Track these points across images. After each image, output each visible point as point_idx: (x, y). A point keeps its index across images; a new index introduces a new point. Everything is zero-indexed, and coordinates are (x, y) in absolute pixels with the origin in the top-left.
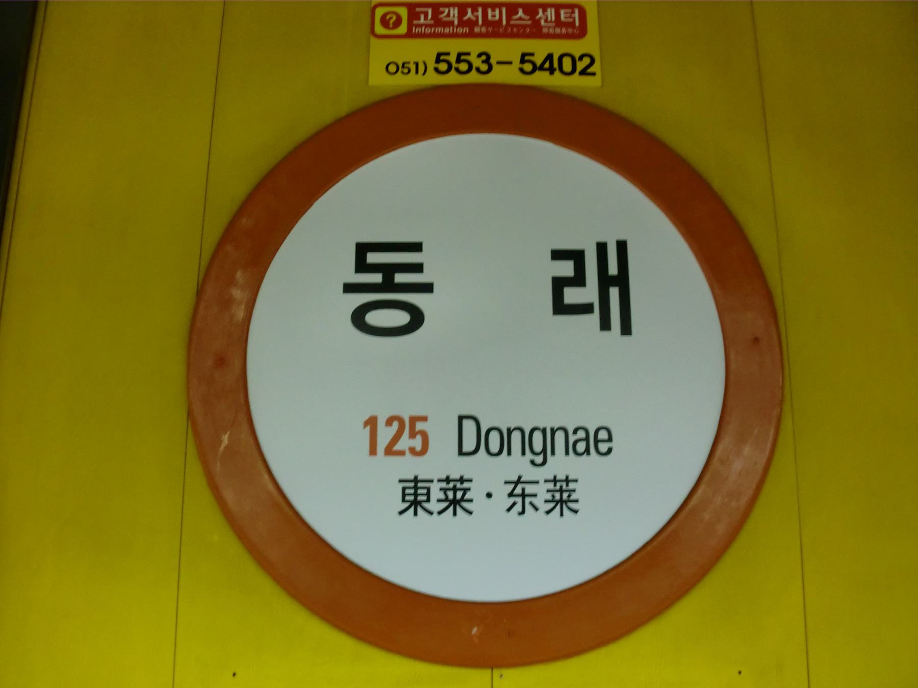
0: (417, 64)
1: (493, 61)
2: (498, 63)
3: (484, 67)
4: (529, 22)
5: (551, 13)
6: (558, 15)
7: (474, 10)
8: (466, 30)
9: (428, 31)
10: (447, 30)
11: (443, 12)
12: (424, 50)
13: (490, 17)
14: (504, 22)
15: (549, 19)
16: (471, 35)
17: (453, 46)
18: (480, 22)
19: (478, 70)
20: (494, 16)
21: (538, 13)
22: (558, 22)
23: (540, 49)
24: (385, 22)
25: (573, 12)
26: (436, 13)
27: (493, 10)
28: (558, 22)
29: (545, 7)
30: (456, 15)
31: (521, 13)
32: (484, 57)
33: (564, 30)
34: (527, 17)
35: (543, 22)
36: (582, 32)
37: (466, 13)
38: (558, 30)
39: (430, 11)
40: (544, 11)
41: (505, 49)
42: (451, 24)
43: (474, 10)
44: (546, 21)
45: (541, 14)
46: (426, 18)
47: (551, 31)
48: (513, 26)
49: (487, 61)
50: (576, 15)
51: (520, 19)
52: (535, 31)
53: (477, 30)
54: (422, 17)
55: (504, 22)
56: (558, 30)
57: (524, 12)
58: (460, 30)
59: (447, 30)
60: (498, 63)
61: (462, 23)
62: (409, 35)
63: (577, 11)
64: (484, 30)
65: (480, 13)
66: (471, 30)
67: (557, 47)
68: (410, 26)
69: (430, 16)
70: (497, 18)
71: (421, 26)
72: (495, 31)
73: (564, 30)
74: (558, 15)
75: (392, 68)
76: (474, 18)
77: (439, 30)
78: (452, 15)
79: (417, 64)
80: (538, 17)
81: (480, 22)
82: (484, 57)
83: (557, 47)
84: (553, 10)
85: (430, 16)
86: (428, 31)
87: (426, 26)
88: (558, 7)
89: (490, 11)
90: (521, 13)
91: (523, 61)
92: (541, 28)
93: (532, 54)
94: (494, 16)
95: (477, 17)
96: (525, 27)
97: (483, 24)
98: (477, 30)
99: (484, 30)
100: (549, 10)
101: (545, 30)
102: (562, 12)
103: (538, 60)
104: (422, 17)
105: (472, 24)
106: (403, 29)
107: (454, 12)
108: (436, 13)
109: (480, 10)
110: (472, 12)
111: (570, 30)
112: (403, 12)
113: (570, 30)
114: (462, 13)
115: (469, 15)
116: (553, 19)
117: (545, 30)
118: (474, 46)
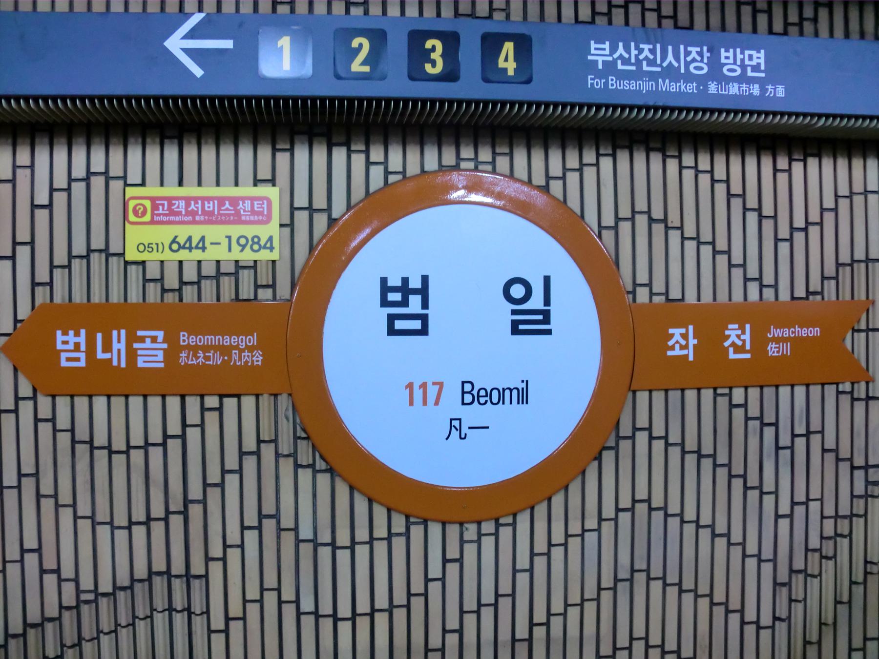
5: (248, 204)
6: (252, 205)
7: (196, 203)
8: (190, 218)
9: (165, 219)
10: (178, 219)
13: (207, 209)
16: (194, 222)
18: (200, 213)
22: (253, 212)
24: (136, 213)
26: (170, 205)
28: (253, 212)
29: (244, 199)
31: (227, 205)
38: (252, 218)
39: (166, 203)
43: (196, 203)
44: (244, 211)
45: (241, 206)
46: (163, 209)
47: (248, 218)
48: (222, 215)
51: (227, 209)
52: (237, 219)
53: (197, 218)
54: (161, 207)
56: (252, 218)
57: (230, 205)
58: (186, 219)
59: (178, 219)
61: (188, 213)
62: (152, 222)
64: (202, 218)
65: (199, 205)
66: (194, 218)
67: (249, 231)
68: (153, 215)
70: (211, 209)
71: (159, 215)
72: (211, 219)
74: (252, 205)
75: (141, 248)
77: (172, 218)
79: (157, 244)
81: (200, 213)
83: (249, 231)
86: (165, 219)
87: (164, 215)
90: (227, 205)
92: (240, 215)
94: (209, 207)
95: (197, 208)
96: (229, 215)
97: (202, 214)
98: (197, 218)
99: (202, 218)
101: (243, 218)
102: (255, 203)
104: (161, 207)
105: (194, 213)
106: (147, 218)
107: (182, 204)
108: (170, 205)
109: (200, 202)
112: (148, 204)
114: (188, 205)
115: (193, 206)
117: (243, 218)
118: (196, 232)
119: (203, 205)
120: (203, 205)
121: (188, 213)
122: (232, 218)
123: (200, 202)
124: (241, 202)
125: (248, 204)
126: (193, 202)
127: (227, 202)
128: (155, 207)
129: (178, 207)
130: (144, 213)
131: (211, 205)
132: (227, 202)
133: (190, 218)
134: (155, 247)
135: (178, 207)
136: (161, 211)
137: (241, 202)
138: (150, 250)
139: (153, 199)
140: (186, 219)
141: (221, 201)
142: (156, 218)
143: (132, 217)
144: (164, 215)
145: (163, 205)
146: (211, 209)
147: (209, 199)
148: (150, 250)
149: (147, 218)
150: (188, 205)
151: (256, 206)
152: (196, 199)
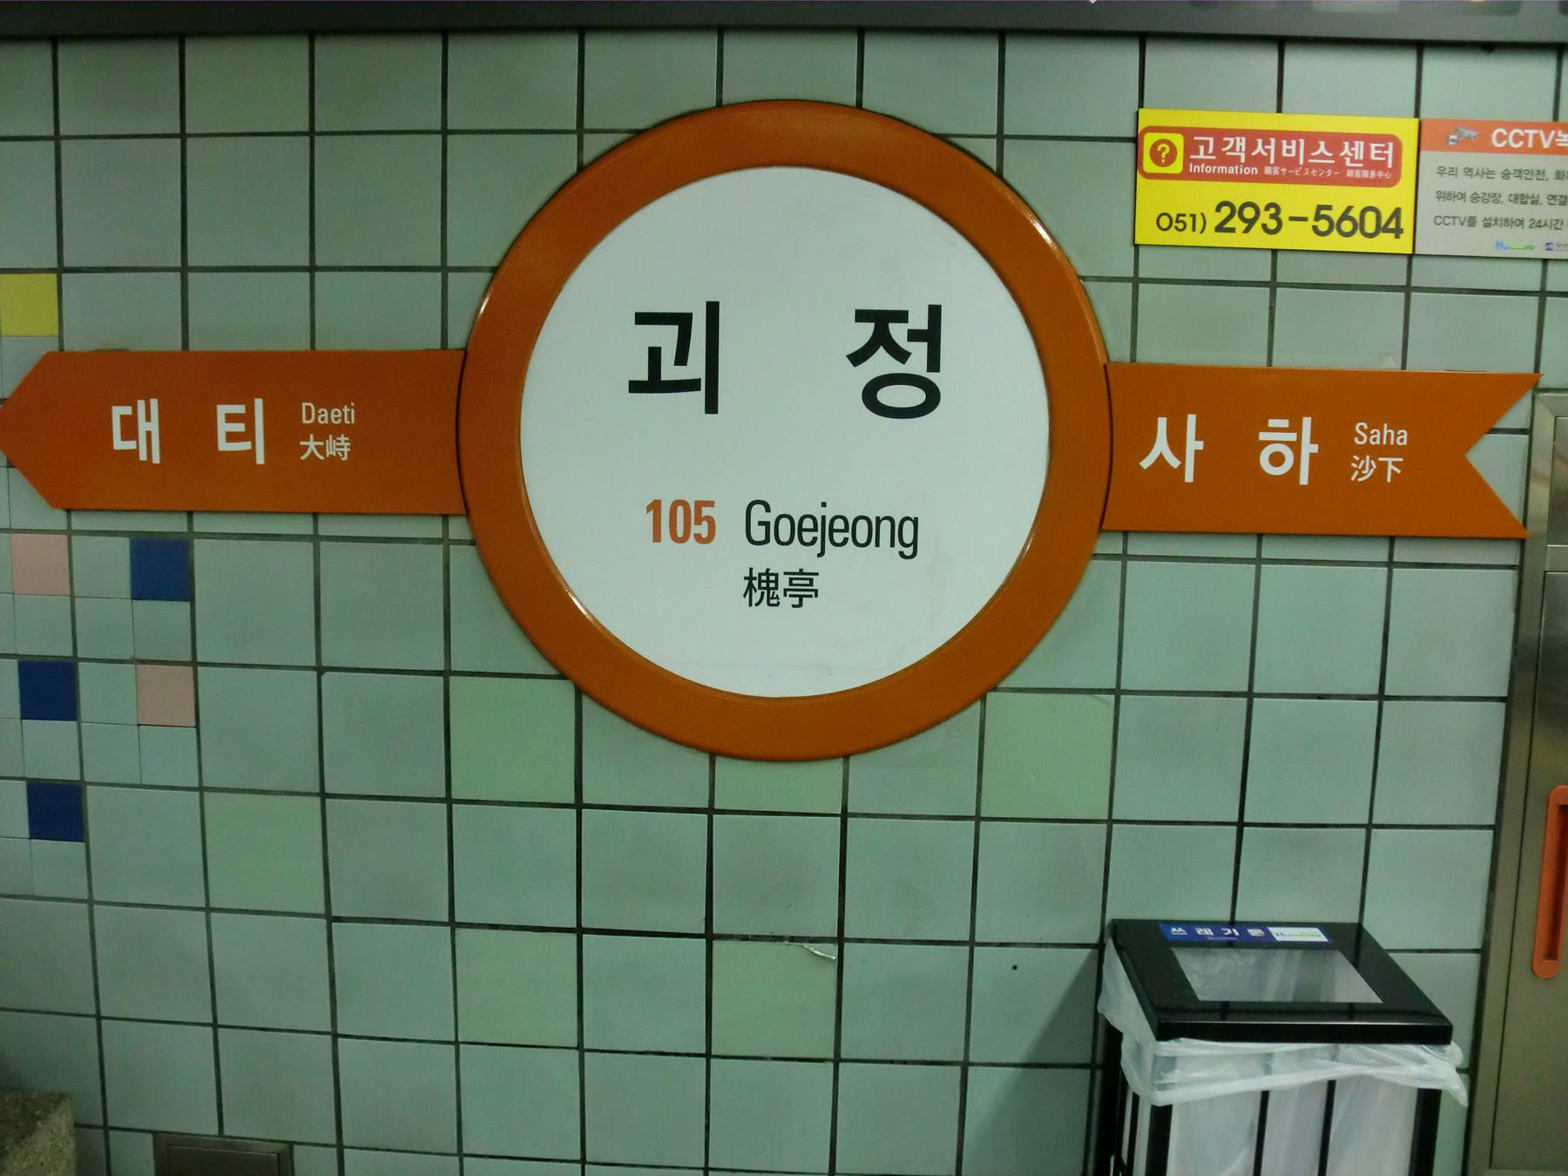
0: (1194, 216)
1: (1284, 216)
2: (1292, 219)
3: (1272, 225)
5: (1359, 146)
6: (1367, 151)
7: (1266, 142)
8: (1255, 170)
9: (1209, 170)
10: (1232, 170)
12: (1203, 197)
13: (1285, 154)
16: (1261, 178)
17: (1238, 193)
19: (1264, 227)
20: (1289, 151)
21: (1342, 149)
23: (1339, 198)
24: (1155, 156)
25: (1386, 148)
26: (1220, 144)
28: (1368, 164)
29: (1352, 138)
31: (1322, 149)
32: (1273, 211)
33: (1373, 174)
35: (1348, 163)
36: (1393, 179)
37: (1255, 147)
38: (1365, 174)
39: (1211, 140)
40: (1352, 145)
41: (1298, 199)
42: (1235, 161)
43: (1266, 142)
44: (1353, 160)
45: (1346, 151)
46: (1206, 153)
47: (1358, 175)
48: (1312, 166)
49: (1275, 217)
50: (1390, 152)
51: (1322, 156)
52: (1339, 177)
53: (1268, 171)
54: (1202, 148)
56: (1365, 174)
58: (1247, 171)
59: (1232, 170)
60: (1292, 219)
61: (1251, 161)
62: (1185, 175)
63: (1391, 145)
65: (1272, 147)
66: (1261, 170)
68: (1187, 161)
72: (1291, 173)
73: (1373, 174)
74: (1367, 151)
75: (1165, 222)
79: (1194, 216)
82: (1273, 211)
87: (1208, 162)
90: (1322, 149)
91: (1318, 217)
93: (1329, 208)
94: (1289, 151)
95: (1268, 151)
97: (1276, 164)
98: (1268, 171)
99: (1276, 171)
101: (1350, 173)
102: (1373, 146)
103: (1335, 215)
104: (1202, 148)
105: (1261, 161)
106: (1177, 167)
107: (1241, 143)
108: (1220, 144)
109: (1273, 140)
111: (1380, 174)
112: (1178, 140)
113: (1380, 174)
114: (1251, 146)
115: (1260, 149)
117: (1350, 173)
118: (1261, 193)
121: (1251, 161)
122: (1329, 172)
123: (1273, 140)
124: (1347, 144)
125: (1359, 146)
126: (1260, 141)
127: (1322, 144)
128: (1191, 147)
129: (1233, 149)
130: (1171, 158)
131: (1293, 147)
132: (1322, 144)
133: (1255, 170)
134: (1189, 220)
136: (1202, 156)
137: (1347, 144)
138: (1181, 226)
139: (1188, 133)
140: (1247, 171)
141: (1312, 139)
142: (1193, 168)
143: (1149, 165)
144: (1208, 162)
145: (1206, 144)
147: (1290, 136)
148: (1181, 226)
149: (1177, 167)
150: (1251, 146)
151: (1373, 152)
152: (1266, 135)
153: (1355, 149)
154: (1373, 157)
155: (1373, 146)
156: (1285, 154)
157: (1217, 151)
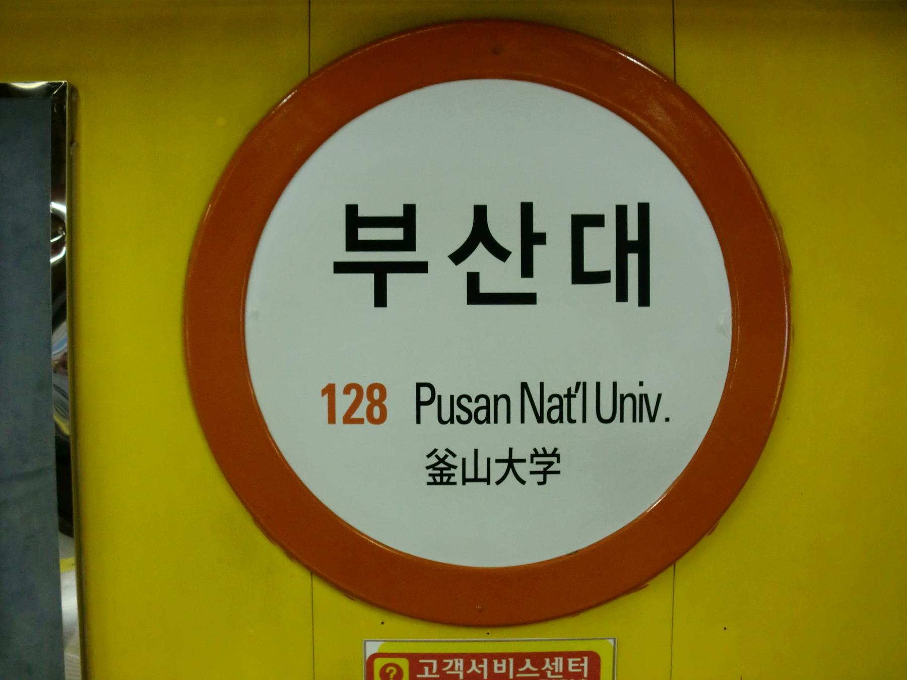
4: (538, 675)
7: (479, 662)
11: (447, 664)
13: (496, 671)
14: (511, 677)
15: (557, 671)
21: (544, 664)
25: (582, 661)
27: (500, 662)
30: (462, 669)
31: (528, 664)
34: (535, 669)
39: (435, 662)
40: (552, 661)
43: (479, 662)
44: (553, 673)
45: (547, 665)
50: (585, 665)
51: (528, 671)
54: (426, 669)
55: (511, 677)
65: (485, 666)
69: (434, 670)
70: (504, 671)
76: (479, 672)
78: (456, 668)
80: (543, 669)
84: (561, 659)
85: (434, 670)
88: (566, 655)
89: (496, 662)
90: (528, 664)
95: (482, 669)
100: (556, 659)
102: (570, 660)
104: (426, 669)
107: (460, 663)
108: (441, 665)
109: (485, 661)
110: (477, 666)
114: (467, 665)
115: (474, 667)
116: (561, 670)
119: (490, 666)
120: (490, 666)
123: (485, 661)
124: (547, 660)
126: (474, 662)
127: (528, 661)
129: (453, 668)
131: (504, 665)
132: (528, 661)
135: (453, 668)
137: (547, 660)
145: (430, 666)
146: (504, 671)
150: (467, 665)
151: (571, 665)
152: (479, 657)
153: (556, 664)
154: (570, 669)
155: (570, 660)
156: (496, 671)
157: (439, 671)
